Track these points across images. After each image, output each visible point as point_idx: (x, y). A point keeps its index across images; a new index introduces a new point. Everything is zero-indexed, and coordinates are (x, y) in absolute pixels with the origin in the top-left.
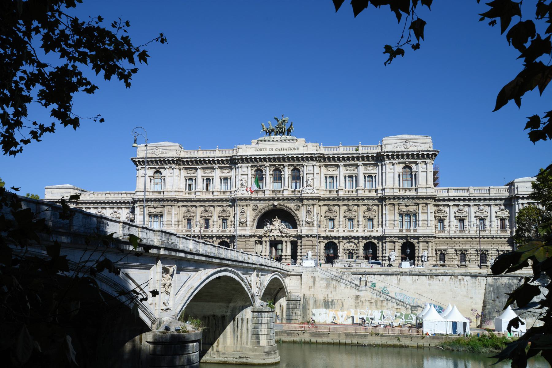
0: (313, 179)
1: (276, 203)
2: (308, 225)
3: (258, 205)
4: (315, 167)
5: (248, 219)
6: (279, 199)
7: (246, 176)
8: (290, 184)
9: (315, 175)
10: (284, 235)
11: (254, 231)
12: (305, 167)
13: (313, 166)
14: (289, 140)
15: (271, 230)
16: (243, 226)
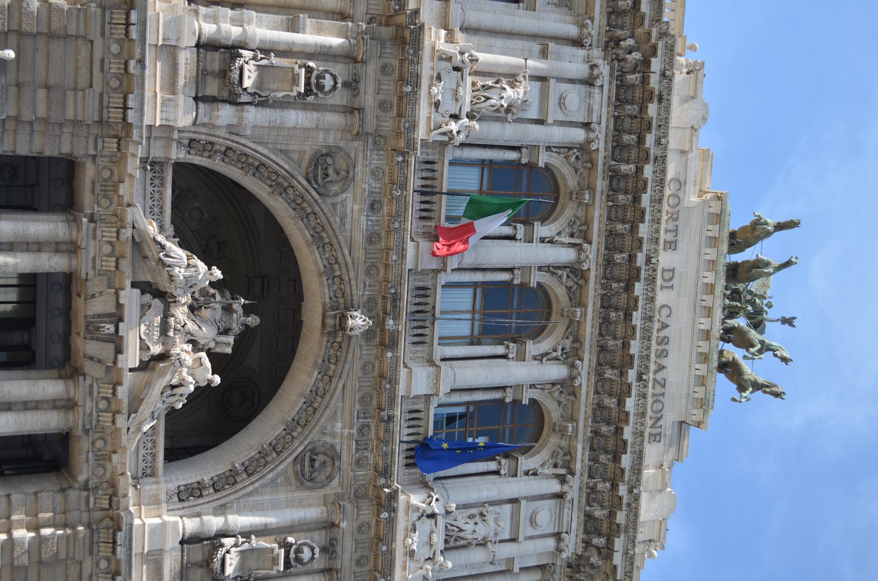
0: (483, 544)
1: (358, 321)
2: (197, 553)
3: (348, 196)
4: (551, 543)
5: (253, 115)
6: (382, 339)
7: (533, 114)
8: (466, 398)
9: (506, 551)
10: (122, 392)
11: (157, 152)
12: (554, 487)
13: (558, 536)
14: (702, 381)
15: (160, 294)
16: (201, 75)
